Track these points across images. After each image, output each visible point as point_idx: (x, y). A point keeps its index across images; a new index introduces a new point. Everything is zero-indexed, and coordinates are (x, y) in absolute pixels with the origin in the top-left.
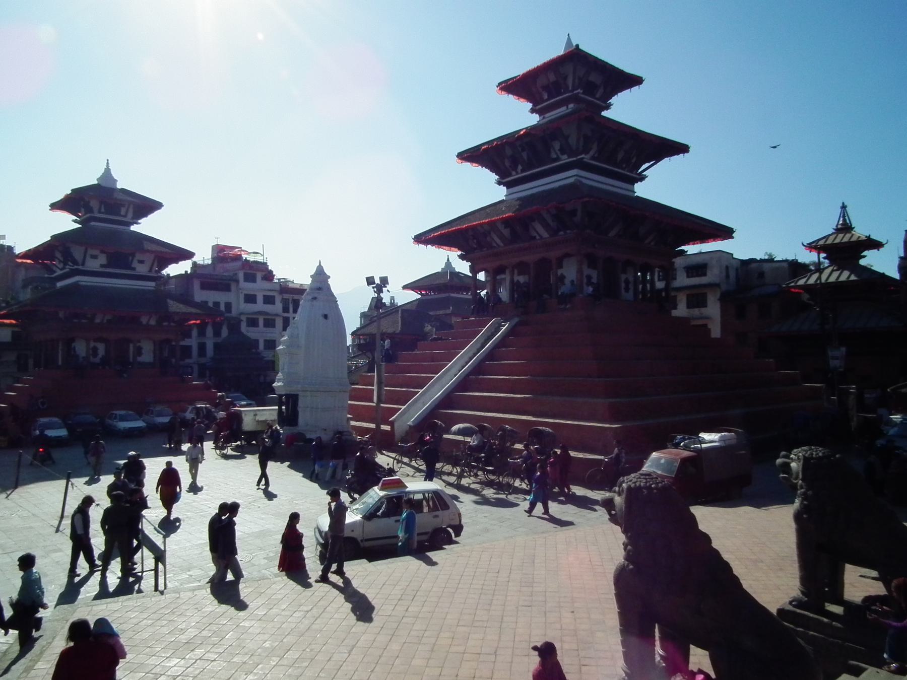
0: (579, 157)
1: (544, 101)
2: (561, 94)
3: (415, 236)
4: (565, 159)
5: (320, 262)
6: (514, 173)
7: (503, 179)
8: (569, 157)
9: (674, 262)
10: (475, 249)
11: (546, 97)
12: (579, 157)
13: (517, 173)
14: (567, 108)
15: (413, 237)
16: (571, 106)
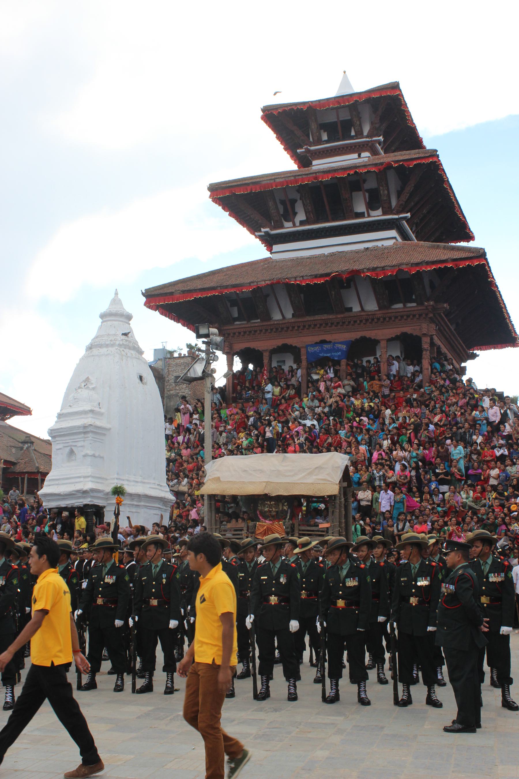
0: (401, 216)
1: (319, 141)
2: (352, 138)
3: (146, 290)
4: (377, 215)
5: (116, 294)
6: (289, 224)
7: (271, 230)
8: (384, 214)
9: (464, 369)
10: (236, 320)
11: (325, 137)
12: (401, 216)
13: (294, 225)
14: (359, 156)
15: (144, 292)
16: (366, 154)
